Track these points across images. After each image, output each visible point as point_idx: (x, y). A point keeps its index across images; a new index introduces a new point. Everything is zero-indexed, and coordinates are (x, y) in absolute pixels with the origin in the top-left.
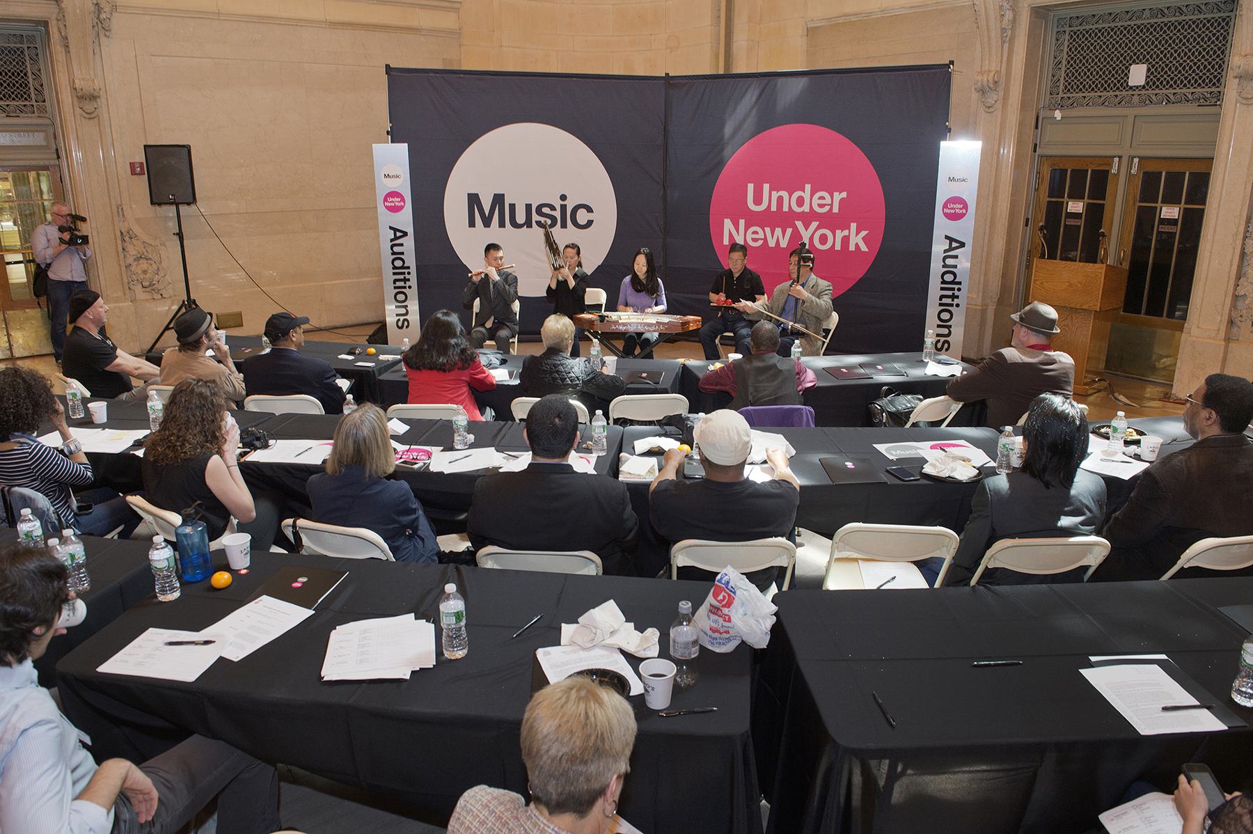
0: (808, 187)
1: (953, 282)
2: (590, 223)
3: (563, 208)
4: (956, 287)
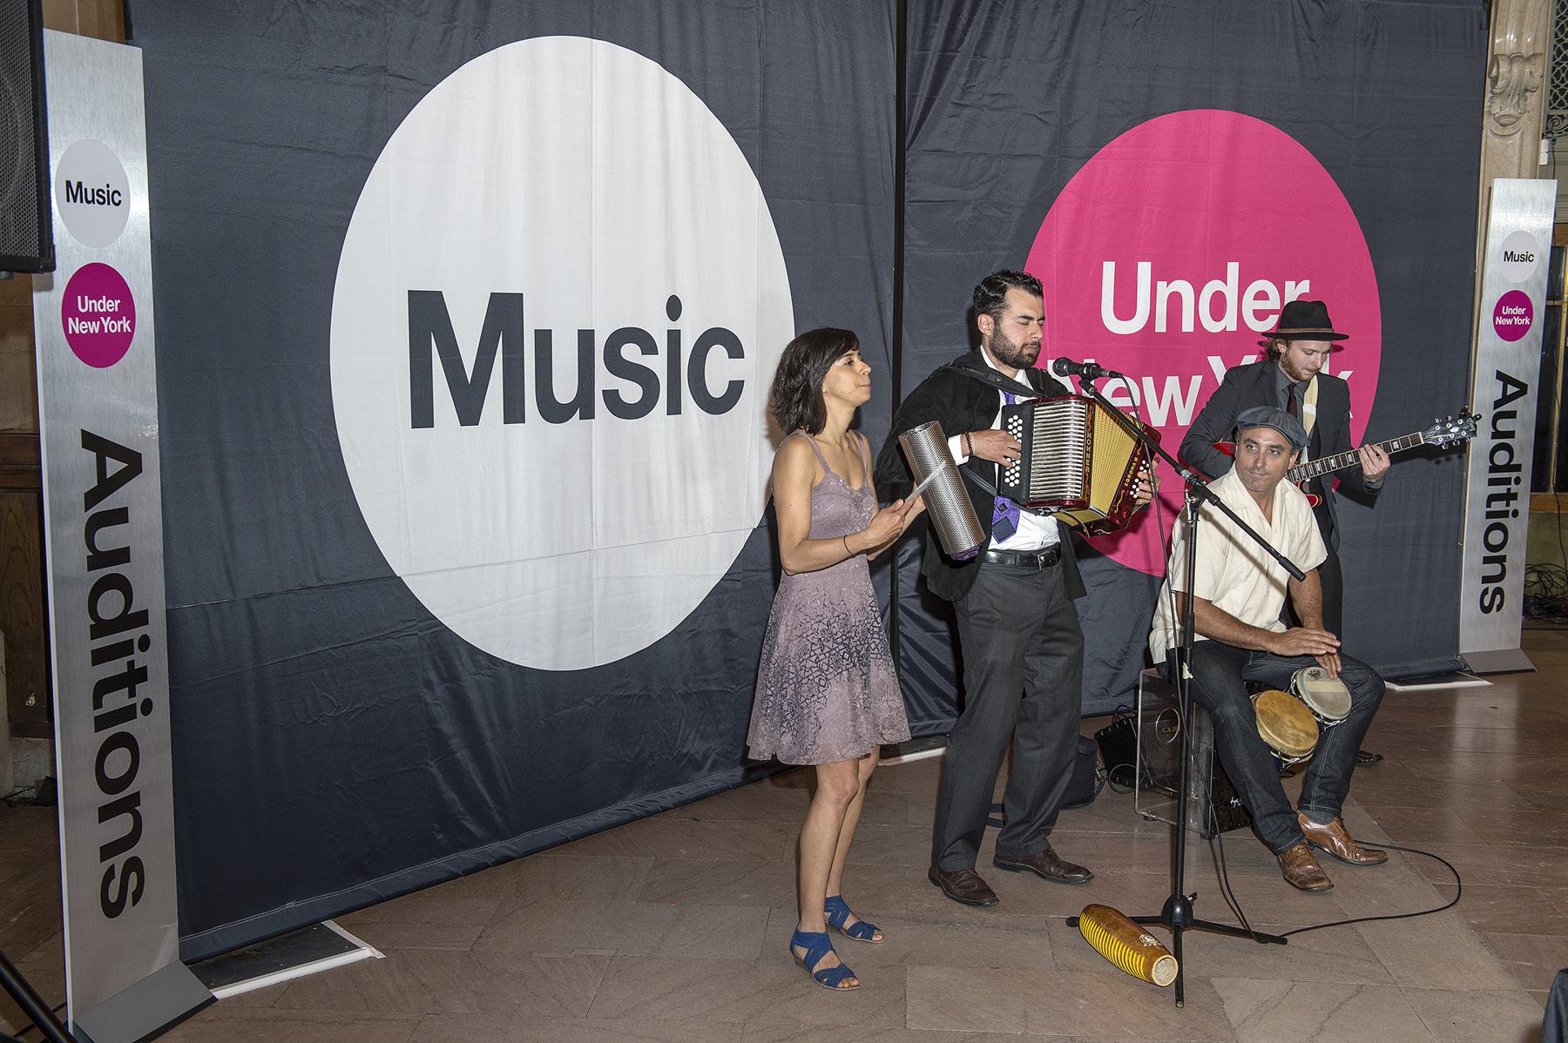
0: (1233, 269)
1: (1509, 467)
2: (736, 388)
3: (674, 337)
4: (1513, 475)
